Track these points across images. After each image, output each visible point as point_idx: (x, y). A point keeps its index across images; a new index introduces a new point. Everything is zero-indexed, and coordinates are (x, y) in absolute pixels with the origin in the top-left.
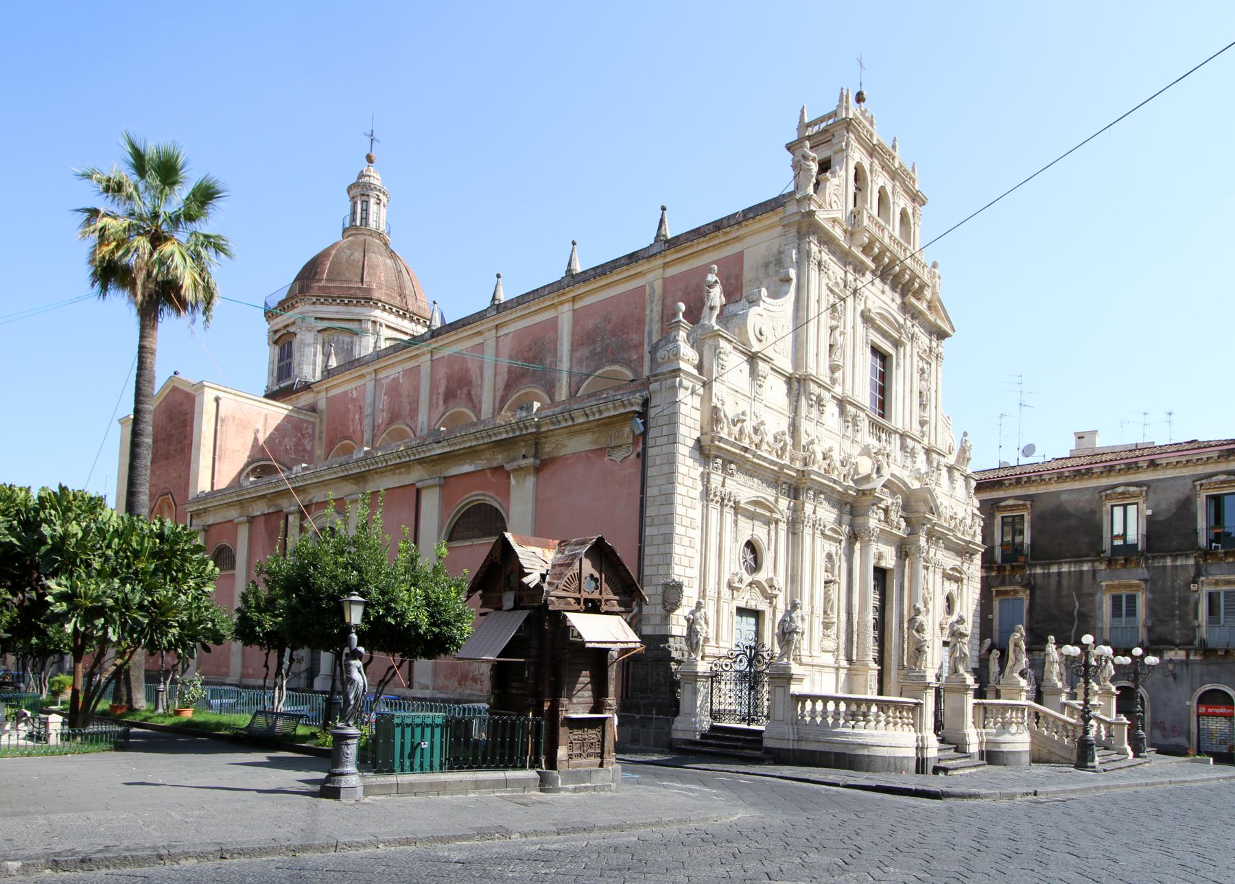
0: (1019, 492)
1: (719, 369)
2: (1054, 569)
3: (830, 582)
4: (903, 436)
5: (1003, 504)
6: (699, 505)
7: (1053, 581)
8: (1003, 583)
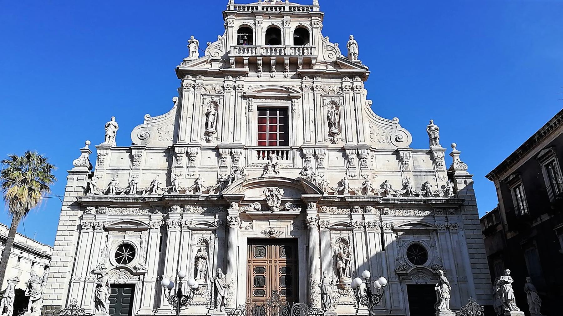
0: (547, 142)
1: (99, 163)
3: (202, 257)
4: (300, 149)
5: (540, 156)
6: (76, 234)
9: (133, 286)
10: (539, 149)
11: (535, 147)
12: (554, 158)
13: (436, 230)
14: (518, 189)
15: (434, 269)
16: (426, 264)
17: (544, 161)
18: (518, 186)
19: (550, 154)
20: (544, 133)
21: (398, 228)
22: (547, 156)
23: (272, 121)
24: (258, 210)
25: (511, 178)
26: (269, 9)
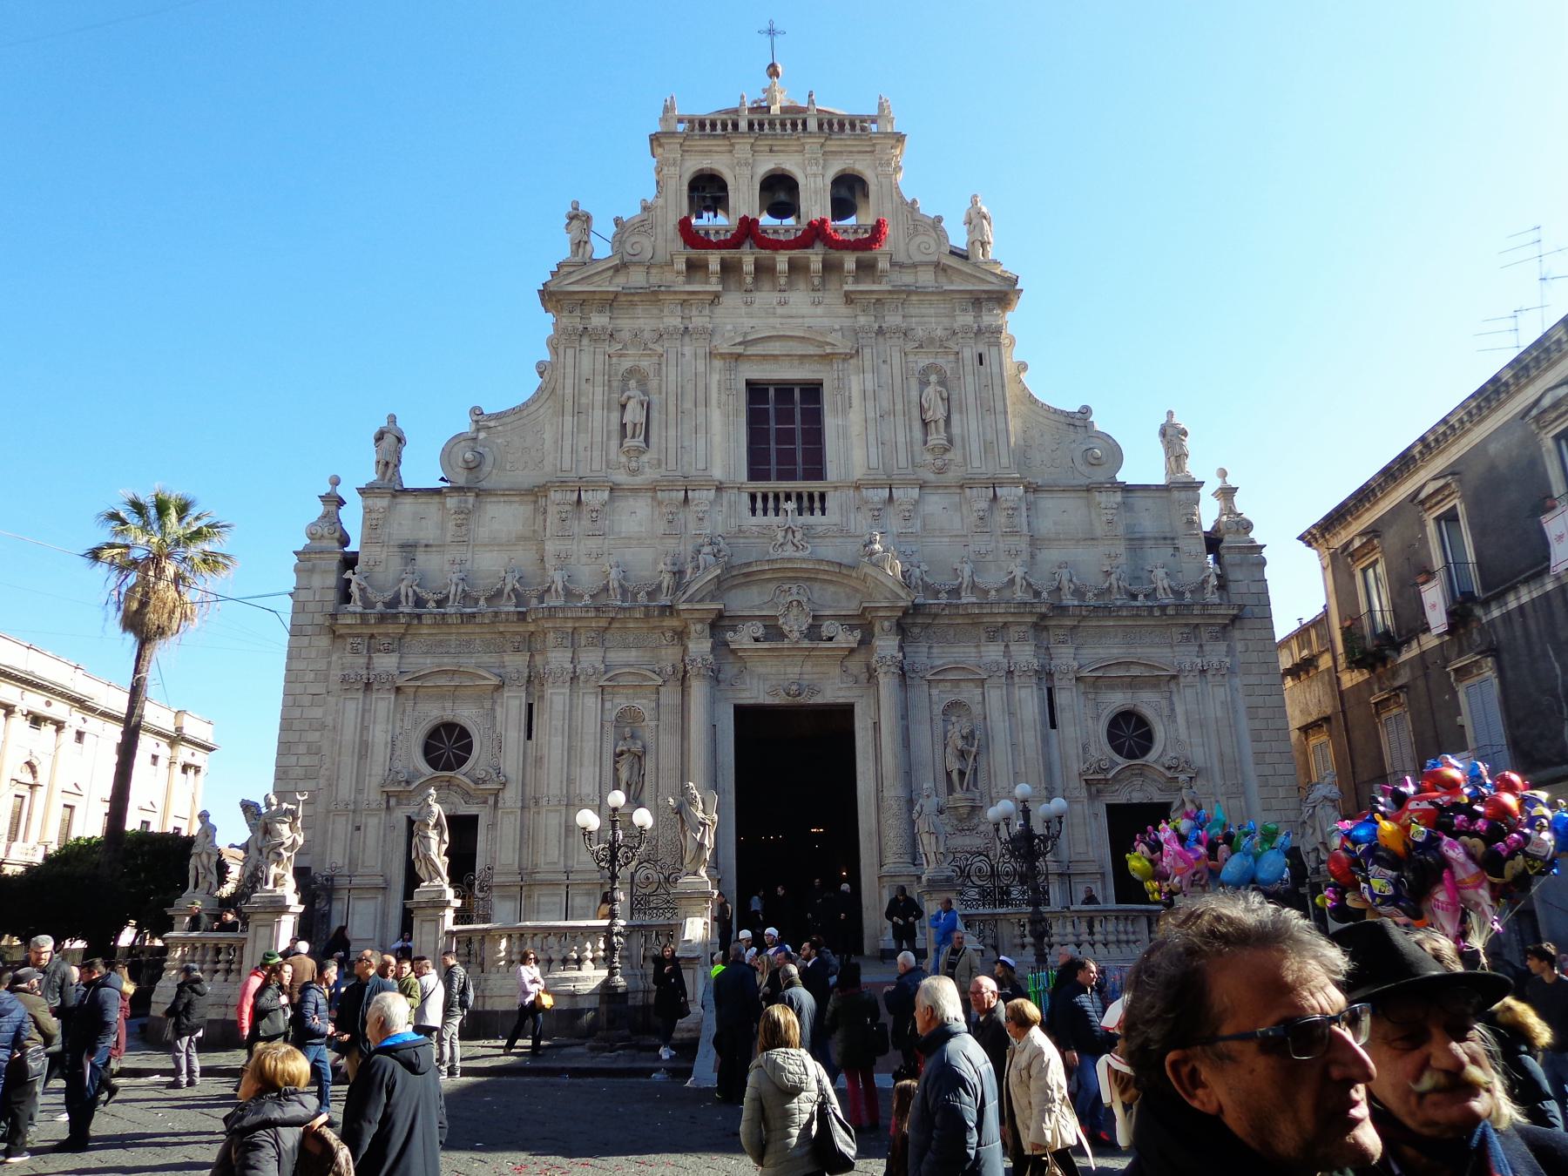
0: (1440, 463)
2: (1512, 603)
5: (1423, 495)
7: (1517, 620)
8: (1460, 654)
9: (474, 819)
10: (1422, 478)
11: (1417, 470)
12: (1456, 501)
13: (1174, 677)
14: (1371, 571)
15: (1169, 768)
16: (1152, 756)
17: (1430, 508)
18: (1374, 564)
19: (1446, 493)
20: (1437, 440)
21: (1089, 674)
22: (1440, 497)
23: (785, 416)
24: (757, 640)
25: (1357, 544)
26: (766, 126)
